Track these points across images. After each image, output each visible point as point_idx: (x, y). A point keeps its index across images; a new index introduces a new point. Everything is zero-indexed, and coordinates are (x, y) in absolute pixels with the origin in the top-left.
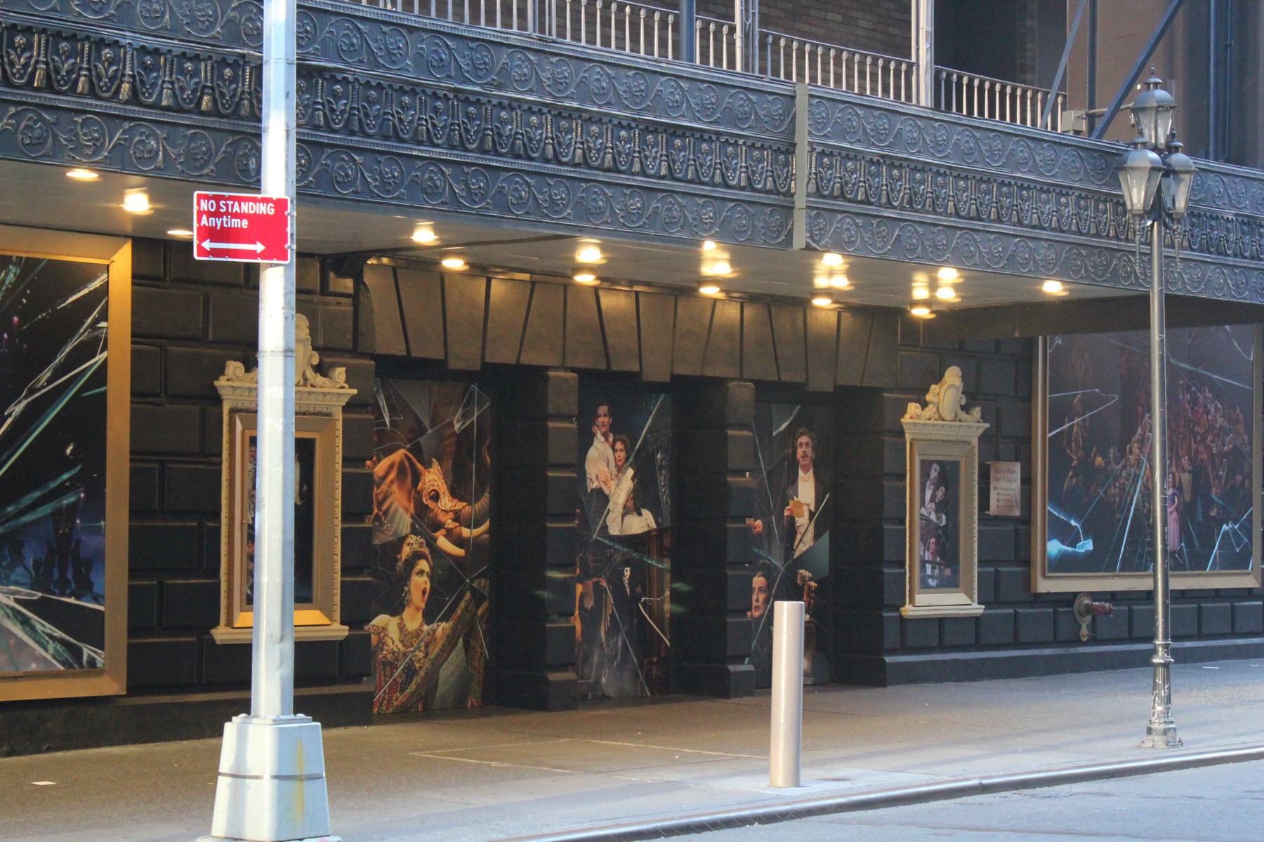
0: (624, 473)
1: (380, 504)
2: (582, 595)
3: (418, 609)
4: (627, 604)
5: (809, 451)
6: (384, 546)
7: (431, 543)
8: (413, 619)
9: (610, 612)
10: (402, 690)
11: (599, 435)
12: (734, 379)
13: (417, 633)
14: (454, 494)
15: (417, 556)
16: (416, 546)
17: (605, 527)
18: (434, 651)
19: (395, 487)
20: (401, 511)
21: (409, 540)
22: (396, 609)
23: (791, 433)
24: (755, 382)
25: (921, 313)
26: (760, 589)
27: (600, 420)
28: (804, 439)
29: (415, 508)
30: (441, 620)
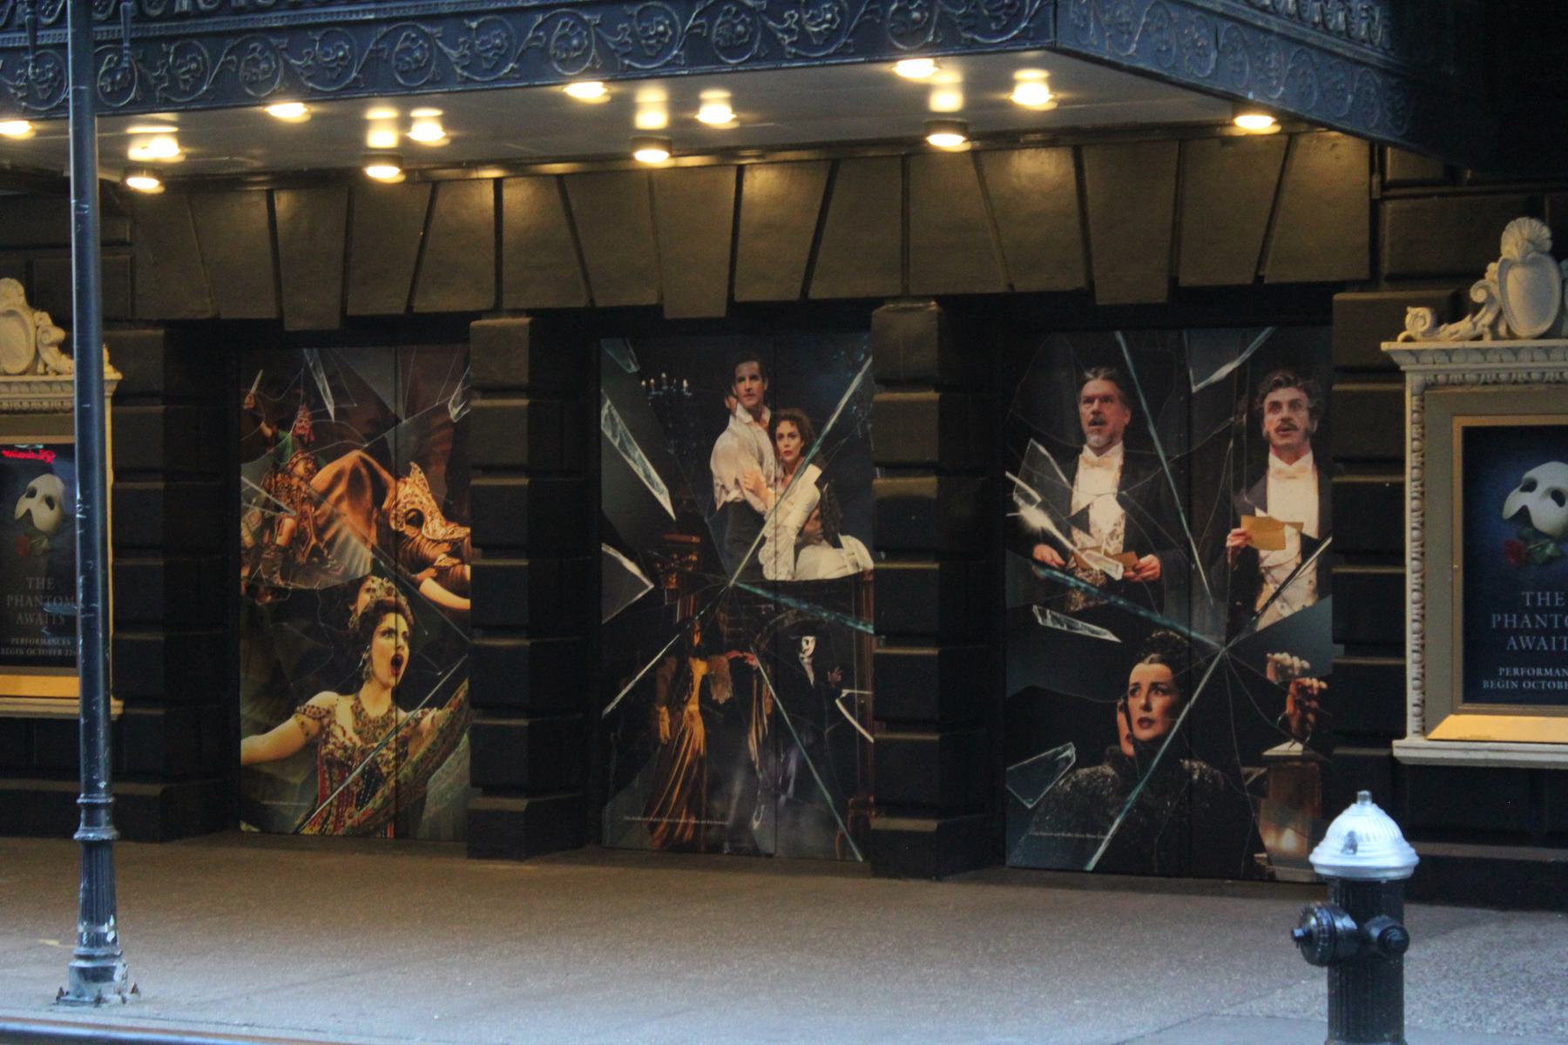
0: (800, 473)
1: (320, 531)
2: (705, 678)
3: (385, 687)
4: (807, 703)
5: (1301, 418)
6: (329, 592)
7: (411, 590)
8: (376, 702)
9: (767, 710)
10: (361, 803)
11: (740, 411)
12: (478, 315)
13: (385, 722)
14: (449, 515)
15: (381, 609)
16: (380, 594)
17: (755, 567)
18: (417, 752)
19: (344, 506)
20: (354, 541)
21: (369, 584)
22: (349, 682)
23: (1249, 385)
24: (938, 299)
25: (385, 174)
26: (1154, 687)
27: (742, 387)
28: (1284, 395)
29: (378, 536)
30: (430, 705)
